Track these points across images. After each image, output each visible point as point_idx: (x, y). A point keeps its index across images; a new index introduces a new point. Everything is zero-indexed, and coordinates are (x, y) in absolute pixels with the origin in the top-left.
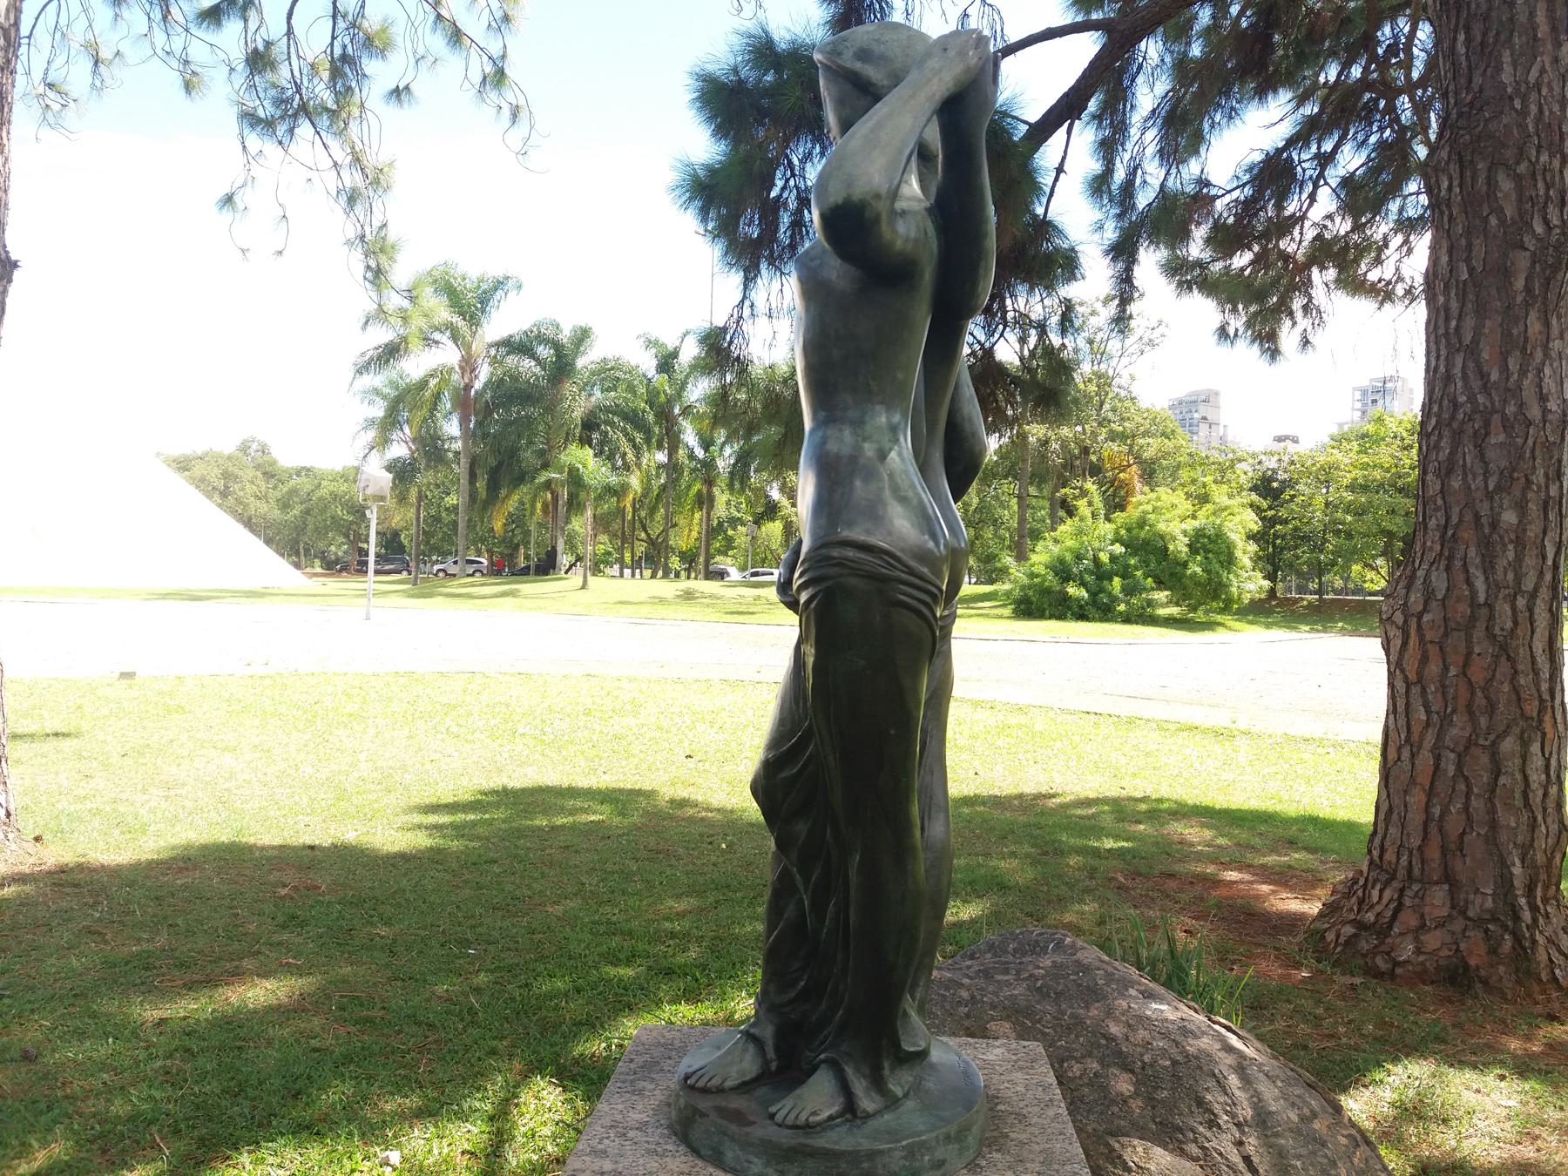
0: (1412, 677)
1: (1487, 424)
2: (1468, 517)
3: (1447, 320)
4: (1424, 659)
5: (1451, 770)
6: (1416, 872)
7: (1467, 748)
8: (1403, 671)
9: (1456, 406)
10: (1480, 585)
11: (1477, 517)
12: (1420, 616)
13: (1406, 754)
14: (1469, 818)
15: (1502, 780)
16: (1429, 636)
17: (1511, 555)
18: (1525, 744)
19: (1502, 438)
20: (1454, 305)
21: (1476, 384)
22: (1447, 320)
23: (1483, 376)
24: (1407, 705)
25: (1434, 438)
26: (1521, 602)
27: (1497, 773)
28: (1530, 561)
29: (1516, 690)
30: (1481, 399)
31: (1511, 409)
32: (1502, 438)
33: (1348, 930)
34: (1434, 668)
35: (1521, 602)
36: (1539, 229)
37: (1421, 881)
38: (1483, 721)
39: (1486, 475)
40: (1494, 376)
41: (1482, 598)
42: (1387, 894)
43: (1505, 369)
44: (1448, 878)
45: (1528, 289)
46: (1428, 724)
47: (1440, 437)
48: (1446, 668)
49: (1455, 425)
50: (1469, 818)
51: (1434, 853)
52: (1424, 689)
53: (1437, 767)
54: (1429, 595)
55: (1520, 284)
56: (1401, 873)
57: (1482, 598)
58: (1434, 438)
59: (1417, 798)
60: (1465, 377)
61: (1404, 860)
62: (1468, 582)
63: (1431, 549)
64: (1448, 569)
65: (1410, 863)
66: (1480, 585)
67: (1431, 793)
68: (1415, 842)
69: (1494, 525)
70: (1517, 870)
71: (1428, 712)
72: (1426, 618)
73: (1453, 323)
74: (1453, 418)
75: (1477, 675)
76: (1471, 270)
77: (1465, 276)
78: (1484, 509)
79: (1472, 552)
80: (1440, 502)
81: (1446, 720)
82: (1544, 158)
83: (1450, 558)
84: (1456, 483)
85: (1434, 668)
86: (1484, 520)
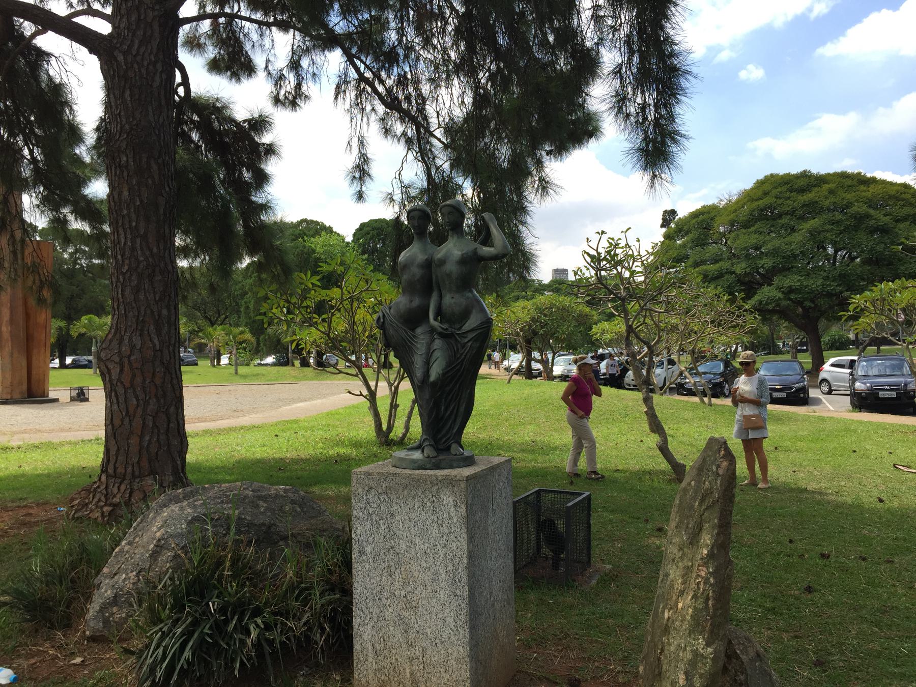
0: (128, 385)
1: (154, 271)
2: (148, 312)
3: (130, 222)
4: (134, 376)
5: (151, 424)
6: (137, 473)
7: (157, 413)
8: (122, 383)
9: (139, 262)
10: (156, 341)
11: (152, 312)
12: (129, 357)
13: (127, 421)
14: (160, 444)
15: (172, 425)
16: (135, 366)
17: (166, 328)
18: (177, 409)
19: (160, 278)
20: (134, 216)
21: (148, 253)
22: (130, 222)
23: (151, 250)
24: (126, 398)
25: (128, 275)
26: (171, 349)
27: (169, 422)
28: (173, 331)
29: (173, 386)
30: (150, 260)
31: (162, 265)
32: (160, 278)
33: (107, 509)
34: (139, 380)
35: (171, 349)
36: (167, 189)
37: (139, 477)
38: (162, 401)
39: (155, 293)
40: (155, 250)
41: (158, 347)
42: (123, 487)
43: (158, 248)
45: (165, 214)
46: (138, 406)
47: (131, 275)
48: (144, 380)
49: (139, 270)
50: (160, 444)
51: (145, 464)
52: (134, 392)
53: (144, 423)
54: (132, 347)
55: (162, 211)
56: (128, 477)
57: (158, 347)
58: (128, 275)
59: (134, 441)
60: (142, 249)
61: (130, 469)
62: (151, 340)
63: (131, 326)
64: (141, 335)
65: (133, 471)
66: (156, 341)
67: (141, 437)
68: (135, 460)
69: (159, 316)
70: (179, 462)
71: (138, 400)
72: (133, 358)
73: (134, 224)
74: (138, 267)
76: (141, 201)
77: (138, 203)
78: (155, 310)
79: (152, 327)
80: (134, 305)
82: (167, 158)
83: (142, 330)
84: (142, 297)
85: (139, 380)
86: (156, 313)
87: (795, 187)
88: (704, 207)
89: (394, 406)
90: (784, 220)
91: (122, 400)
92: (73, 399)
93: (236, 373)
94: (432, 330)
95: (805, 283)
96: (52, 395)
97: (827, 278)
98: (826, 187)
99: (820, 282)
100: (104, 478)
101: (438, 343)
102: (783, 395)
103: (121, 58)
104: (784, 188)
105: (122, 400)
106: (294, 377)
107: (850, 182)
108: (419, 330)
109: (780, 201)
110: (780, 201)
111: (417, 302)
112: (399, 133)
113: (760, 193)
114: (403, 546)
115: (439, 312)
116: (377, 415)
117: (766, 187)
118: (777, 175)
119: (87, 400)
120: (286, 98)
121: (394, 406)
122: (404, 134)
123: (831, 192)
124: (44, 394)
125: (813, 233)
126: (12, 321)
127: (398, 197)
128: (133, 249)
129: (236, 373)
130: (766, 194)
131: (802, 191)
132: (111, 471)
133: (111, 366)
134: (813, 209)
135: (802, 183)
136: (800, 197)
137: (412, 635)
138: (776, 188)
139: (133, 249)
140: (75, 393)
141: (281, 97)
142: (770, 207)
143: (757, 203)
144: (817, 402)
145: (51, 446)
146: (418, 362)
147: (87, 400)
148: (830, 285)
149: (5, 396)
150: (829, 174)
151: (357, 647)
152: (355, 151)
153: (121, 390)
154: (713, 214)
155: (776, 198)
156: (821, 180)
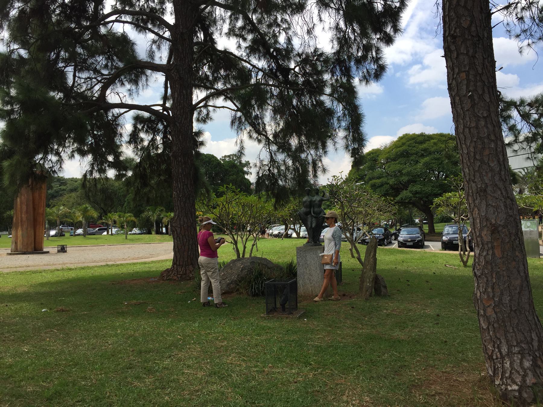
34: (187, 233)
42: (183, 269)
44: (192, 264)
54: (184, 222)
75: (192, 233)
81: (189, 240)
87: (418, 141)
88: (373, 150)
89: (245, 247)
90: (413, 158)
91: (181, 240)
92: (59, 251)
93: (126, 238)
94: (312, 216)
95: (423, 189)
96: (45, 250)
97: (433, 187)
98: (432, 141)
99: (430, 189)
100: (175, 266)
101: (314, 219)
102: (411, 244)
103: (178, 125)
104: (412, 141)
105: (181, 240)
106: (160, 240)
107: (444, 139)
108: (309, 216)
109: (410, 148)
110: (410, 148)
111: (308, 210)
112: (255, 138)
113: (401, 144)
114: (309, 262)
115: (314, 213)
116: (238, 251)
117: (404, 141)
118: (409, 134)
119: (66, 252)
120: (202, 119)
121: (245, 247)
122: (257, 138)
123: (435, 144)
124: (41, 249)
125: (426, 165)
126: (27, 212)
127: (258, 164)
128: (183, 189)
129: (126, 238)
130: (404, 144)
131: (421, 143)
132: (178, 263)
133: (177, 228)
134: (426, 152)
135: (421, 139)
136: (420, 146)
137: (311, 281)
138: (408, 141)
139: (183, 189)
140: (60, 249)
141: (200, 119)
142: (404, 151)
143: (399, 149)
144: (428, 247)
145: (88, 268)
146: (309, 223)
147: (66, 252)
148: (434, 190)
149: (24, 250)
150: (434, 134)
151: (298, 285)
152: (239, 145)
153: (181, 237)
154: (377, 154)
155: (408, 146)
156: (429, 138)
